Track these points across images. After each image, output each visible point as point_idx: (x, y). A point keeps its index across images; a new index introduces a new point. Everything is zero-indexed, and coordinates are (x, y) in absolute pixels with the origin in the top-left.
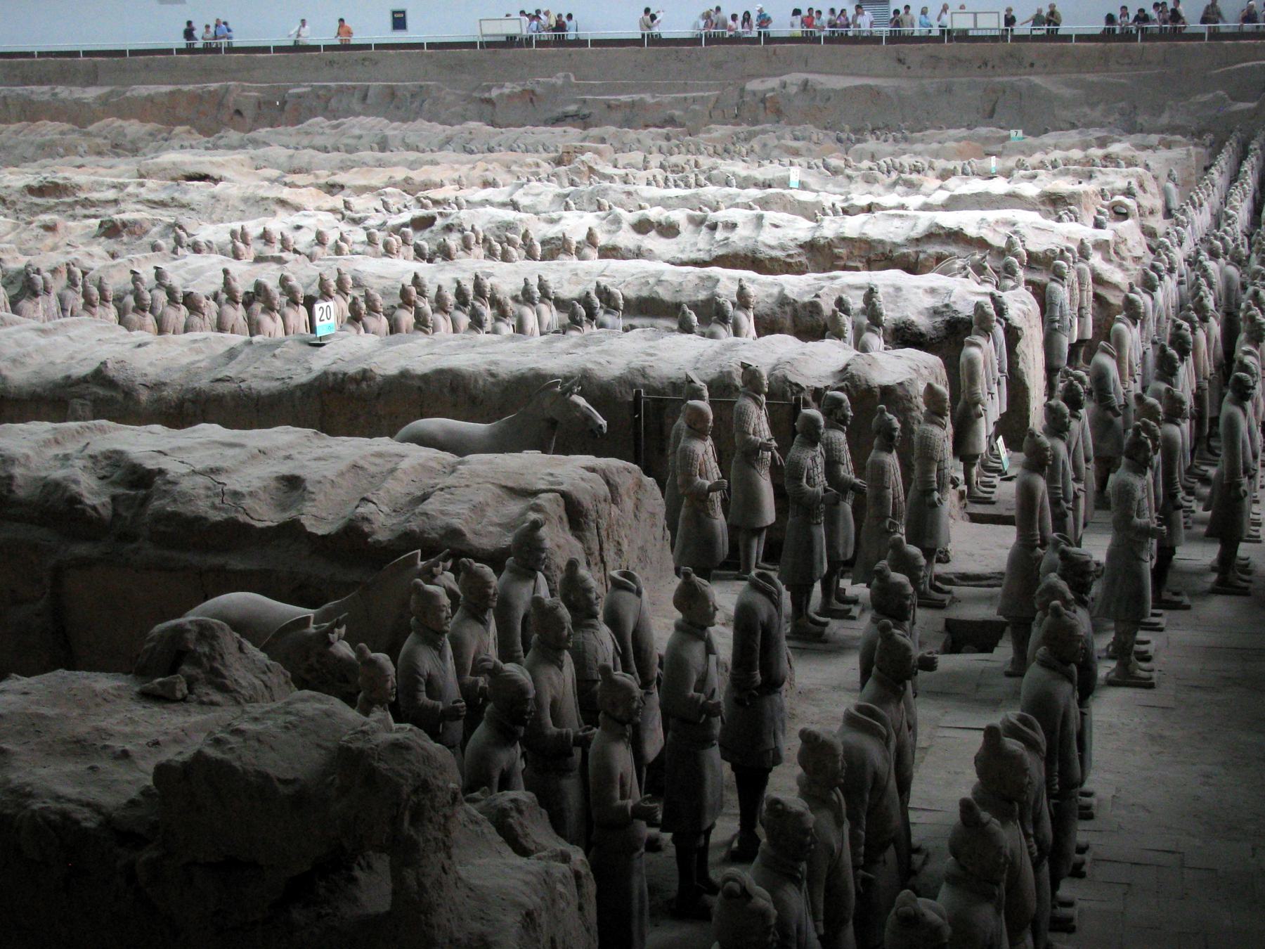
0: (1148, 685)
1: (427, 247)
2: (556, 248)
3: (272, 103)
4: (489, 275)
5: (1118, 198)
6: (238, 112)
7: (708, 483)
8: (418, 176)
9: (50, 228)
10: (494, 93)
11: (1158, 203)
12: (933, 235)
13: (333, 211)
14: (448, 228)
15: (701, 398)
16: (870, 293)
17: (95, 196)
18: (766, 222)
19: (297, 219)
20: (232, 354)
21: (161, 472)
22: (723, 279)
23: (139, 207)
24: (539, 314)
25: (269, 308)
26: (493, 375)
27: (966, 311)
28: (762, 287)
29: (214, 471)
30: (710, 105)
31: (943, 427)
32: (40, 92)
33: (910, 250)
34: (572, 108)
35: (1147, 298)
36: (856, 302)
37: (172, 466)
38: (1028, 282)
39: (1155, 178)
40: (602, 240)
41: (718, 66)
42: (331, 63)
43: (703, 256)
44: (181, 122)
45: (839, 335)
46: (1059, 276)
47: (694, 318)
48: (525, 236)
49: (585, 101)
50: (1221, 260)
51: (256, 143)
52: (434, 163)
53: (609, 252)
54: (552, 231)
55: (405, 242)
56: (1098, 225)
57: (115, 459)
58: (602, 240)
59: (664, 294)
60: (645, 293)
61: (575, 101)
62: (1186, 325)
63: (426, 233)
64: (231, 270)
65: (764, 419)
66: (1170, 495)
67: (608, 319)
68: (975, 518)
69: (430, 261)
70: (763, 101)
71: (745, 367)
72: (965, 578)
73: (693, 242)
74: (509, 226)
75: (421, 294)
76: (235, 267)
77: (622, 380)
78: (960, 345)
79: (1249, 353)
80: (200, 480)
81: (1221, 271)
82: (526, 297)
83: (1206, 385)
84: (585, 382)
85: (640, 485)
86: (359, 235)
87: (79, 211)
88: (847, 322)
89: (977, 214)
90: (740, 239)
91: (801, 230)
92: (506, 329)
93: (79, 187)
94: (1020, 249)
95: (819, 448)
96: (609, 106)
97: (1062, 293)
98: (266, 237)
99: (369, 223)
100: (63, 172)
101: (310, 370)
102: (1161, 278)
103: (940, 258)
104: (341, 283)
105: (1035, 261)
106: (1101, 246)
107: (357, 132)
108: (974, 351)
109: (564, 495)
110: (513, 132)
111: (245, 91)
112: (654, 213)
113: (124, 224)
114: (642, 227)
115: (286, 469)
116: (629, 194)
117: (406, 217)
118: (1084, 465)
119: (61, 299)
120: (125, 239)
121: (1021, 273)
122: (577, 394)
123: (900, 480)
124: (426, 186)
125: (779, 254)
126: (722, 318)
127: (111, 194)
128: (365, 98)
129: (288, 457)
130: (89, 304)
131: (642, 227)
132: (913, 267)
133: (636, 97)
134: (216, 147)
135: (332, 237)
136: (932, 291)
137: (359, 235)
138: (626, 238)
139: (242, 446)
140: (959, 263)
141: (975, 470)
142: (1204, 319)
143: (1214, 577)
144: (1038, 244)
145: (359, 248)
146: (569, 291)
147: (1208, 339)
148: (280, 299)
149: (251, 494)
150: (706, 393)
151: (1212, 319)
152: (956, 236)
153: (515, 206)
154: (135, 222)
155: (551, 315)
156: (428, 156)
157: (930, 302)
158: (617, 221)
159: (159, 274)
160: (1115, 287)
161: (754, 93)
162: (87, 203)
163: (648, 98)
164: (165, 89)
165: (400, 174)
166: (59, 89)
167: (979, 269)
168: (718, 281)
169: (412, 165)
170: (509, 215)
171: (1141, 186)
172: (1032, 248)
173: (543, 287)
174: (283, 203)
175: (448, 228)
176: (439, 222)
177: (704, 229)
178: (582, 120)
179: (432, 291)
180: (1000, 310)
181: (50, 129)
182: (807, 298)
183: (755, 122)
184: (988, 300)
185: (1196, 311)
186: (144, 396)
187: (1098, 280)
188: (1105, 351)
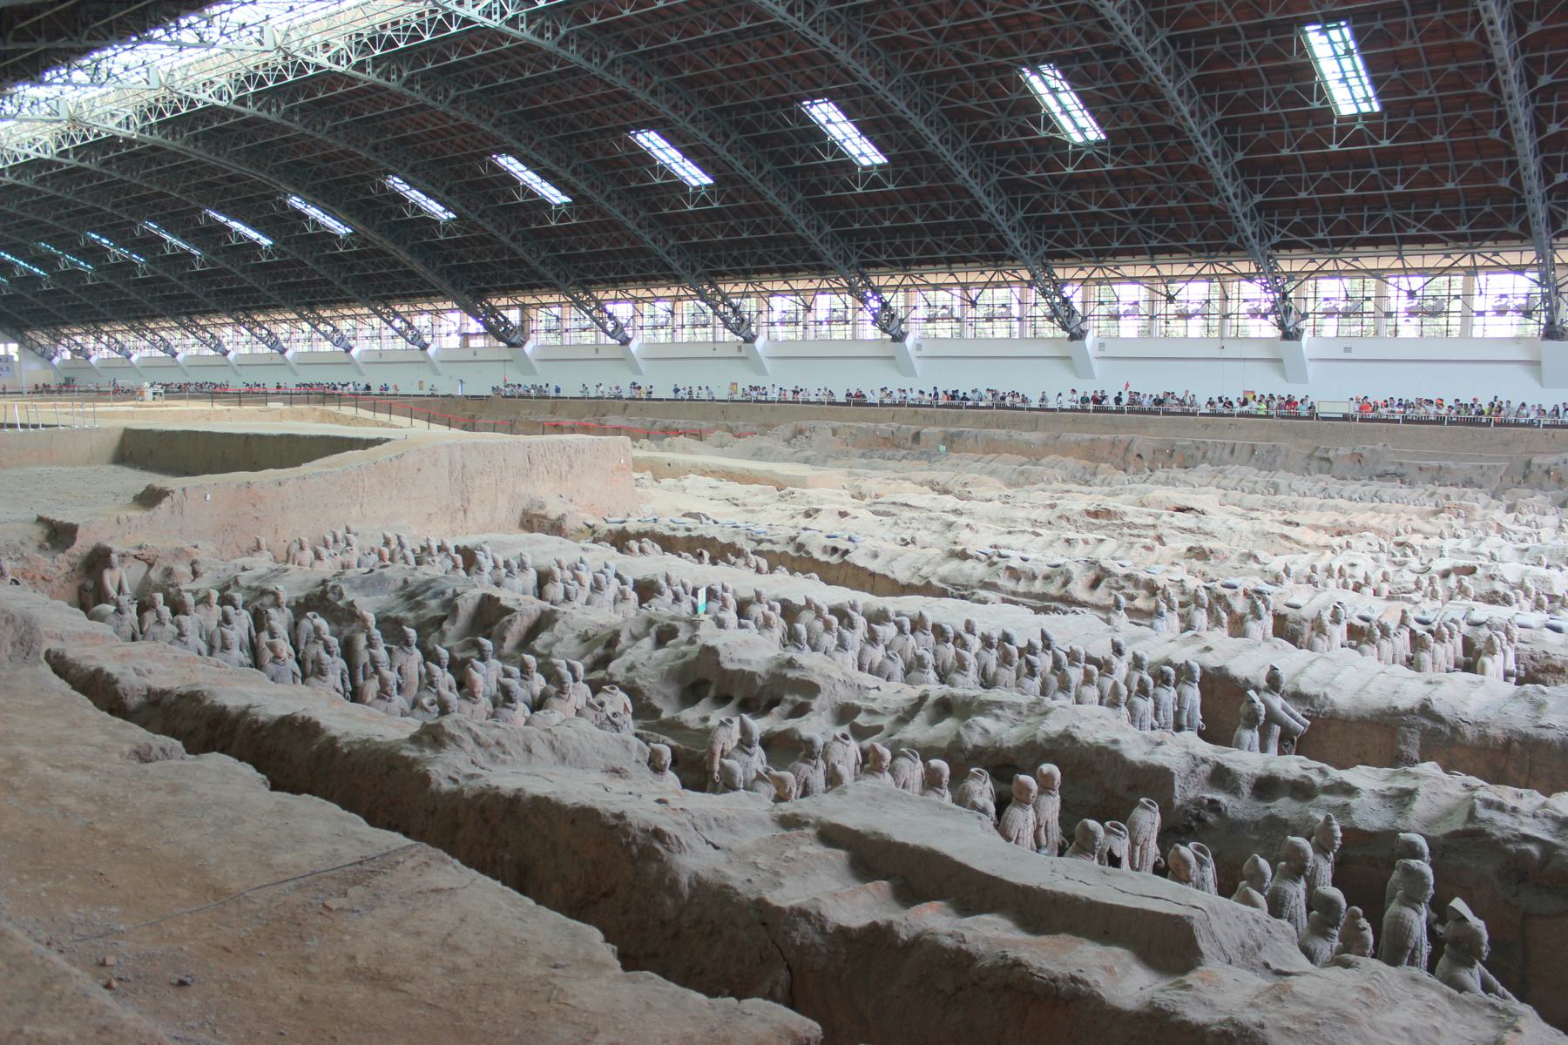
6: (1139, 456)
10: (1331, 454)
17: (1137, 521)
23: (1173, 531)
30: (1502, 473)
34: (1392, 469)
41: (1506, 444)
42: (1206, 426)
44: (1105, 460)
49: (1401, 464)
61: (1393, 463)
70: (1548, 472)
87: (1125, 530)
96: (1421, 469)
100: (1111, 504)
111: (1145, 439)
120: (1212, 562)
127: (1150, 521)
128: (1232, 452)
133: (1443, 464)
161: (1540, 466)
162: (1131, 525)
163: (1451, 464)
164: (1087, 436)
166: (1013, 433)
174: (1286, 537)
176: (1480, 571)
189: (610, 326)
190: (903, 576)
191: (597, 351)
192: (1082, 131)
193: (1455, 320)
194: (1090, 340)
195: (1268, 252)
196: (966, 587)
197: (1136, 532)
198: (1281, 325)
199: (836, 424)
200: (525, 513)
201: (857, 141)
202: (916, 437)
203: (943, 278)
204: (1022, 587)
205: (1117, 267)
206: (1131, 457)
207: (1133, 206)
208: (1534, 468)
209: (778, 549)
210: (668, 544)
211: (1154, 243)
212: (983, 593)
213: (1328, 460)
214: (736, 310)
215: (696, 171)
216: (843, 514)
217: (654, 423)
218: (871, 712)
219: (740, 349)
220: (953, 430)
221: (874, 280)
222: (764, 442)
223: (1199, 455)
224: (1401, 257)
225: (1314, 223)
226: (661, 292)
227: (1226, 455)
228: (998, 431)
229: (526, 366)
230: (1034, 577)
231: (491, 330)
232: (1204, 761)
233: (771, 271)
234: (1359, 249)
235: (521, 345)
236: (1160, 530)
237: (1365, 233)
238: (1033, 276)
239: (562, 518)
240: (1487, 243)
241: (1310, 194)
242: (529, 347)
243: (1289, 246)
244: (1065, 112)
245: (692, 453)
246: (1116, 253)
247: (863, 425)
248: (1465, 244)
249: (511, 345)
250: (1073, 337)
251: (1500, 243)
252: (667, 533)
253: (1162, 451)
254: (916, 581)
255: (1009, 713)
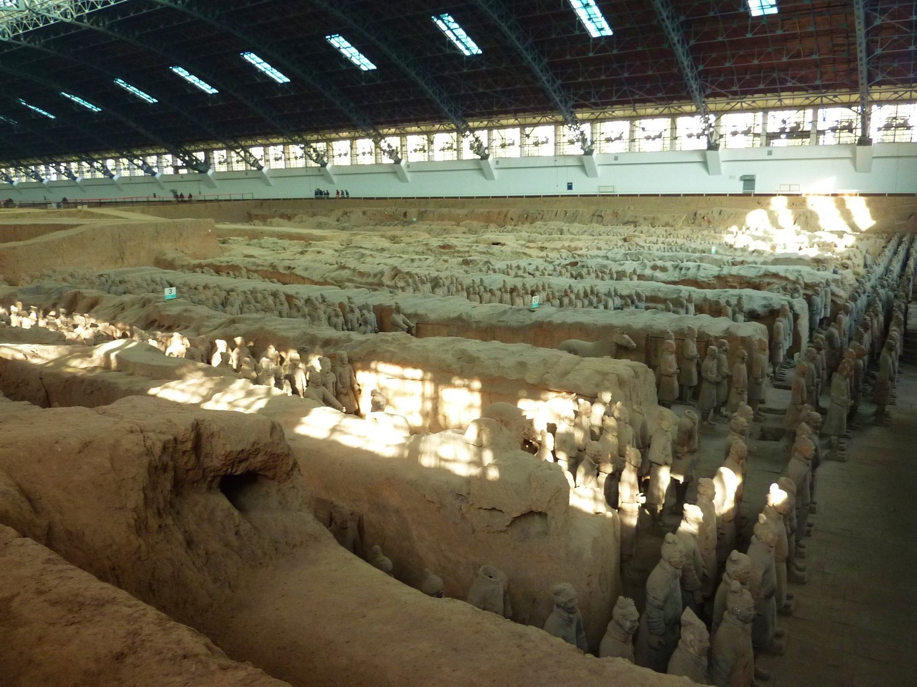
0: (842, 461)
1: (574, 273)
2: (621, 275)
3: (523, 216)
4: (596, 286)
5: (844, 261)
7: (672, 371)
8: (573, 245)
9: (446, 261)
11: (862, 263)
12: (766, 275)
13: (542, 257)
14: (583, 266)
15: (672, 339)
16: (740, 298)
17: (461, 249)
18: (701, 268)
19: (529, 260)
20: (505, 312)
21: (478, 358)
22: (683, 291)
24: (614, 301)
25: (519, 295)
26: (595, 325)
27: (777, 307)
28: (698, 293)
29: (496, 358)
31: (765, 354)
32: (445, 211)
33: (757, 280)
34: (631, 220)
35: (852, 303)
36: (734, 301)
37: (482, 356)
38: (804, 294)
39: (861, 252)
40: (638, 272)
42: (545, 202)
43: (677, 280)
45: (727, 315)
46: (817, 294)
47: (671, 306)
48: (610, 270)
50: (886, 289)
51: (518, 231)
52: (579, 240)
53: (641, 277)
54: (620, 269)
55: (567, 271)
56: (835, 272)
57: (463, 352)
58: (638, 272)
59: (660, 295)
60: (653, 294)
62: (868, 318)
63: (575, 268)
64: (507, 281)
65: (695, 346)
66: (857, 386)
67: (639, 304)
68: (776, 387)
69: (576, 279)
71: (689, 328)
72: (770, 411)
73: (674, 275)
74: (605, 266)
75: (572, 292)
76: (507, 278)
77: (642, 329)
78: (774, 321)
79: (895, 330)
80: (491, 361)
81: (886, 293)
82: (608, 295)
83: (876, 341)
84: (627, 329)
85: (647, 372)
86: (551, 267)
88: (730, 310)
89: (785, 267)
90: (691, 274)
91: (714, 270)
92: (601, 307)
93: (456, 246)
94: (802, 282)
95: (715, 360)
96: (645, 219)
97: (818, 300)
98: (518, 267)
99: (555, 263)
100: (452, 241)
101: (531, 320)
102: (859, 296)
103: (769, 284)
104: (543, 286)
105: (807, 286)
106: (836, 281)
107: (553, 227)
108: (780, 323)
109: (618, 375)
110: (609, 228)
111: (513, 212)
112: (659, 263)
113: (471, 261)
114: (654, 268)
115: (521, 359)
116: (650, 254)
117: (568, 262)
118: (821, 371)
119: (448, 288)
121: (802, 291)
122: (627, 334)
123: (746, 375)
124: (576, 249)
125: (704, 279)
126: (682, 306)
127: (467, 249)
129: (522, 355)
130: (457, 291)
131: (654, 268)
132: (757, 287)
134: (503, 232)
135: (541, 268)
136: (765, 298)
137: (551, 267)
138: (648, 272)
139: (507, 350)
140: (776, 286)
141: (777, 368)
142: (877, 315)
143: (873, 419)
144: (808, 280)
145: (551, 273)
146: (625, 292)
147: (878, 322)
148: (522, 292)
149: (509, 368)
150: (674, 337)
151: (880, 315)
152: (775, 275)
153: (607, 258)
154: (474, 260)
155: (618, 301)
156: (577, 237)
157: (764, 302)
158: (645, 266)
159: (481, 280)
160: (840, 297)
162: (459, 252)
165: (566, 244)
167: (785, 289)
168: (681, 291)
169: (571, 240)
170: (606, 262)
171: (855, 255)
172: (806, 281)
173: (615, 291)
174: (525, 254)
175: (583, 266)
176: (580, 264)
177: (677, 269)
178: (635, 224)
179: (576, 291)
180: (791, 308)
181: (448, 224)
182: (715, 299)
183: (700, 225)
184: (786, 303)
185: (873, 311)
186: (474, 326)
187: (833, 294)
188: (834, 327)
189: (252, 160)
190: (316, 278)
191: (247, 174)
192: (467, 48)
193: (668, 142)
194: (490, 159)
195: (571, 110)
196: (341, 282)
197: (460, 255)
198: (582, 148)
199: (365, 209)
200: (156, 258)
201: (358, 57)
202: (405, 214)
203: (414, 129)
204: (364, 280)
205: (499, 121)
206: (508, 220)
207: (499, 89)
208: (698, 215)
209: (264, 269)
210: (218, 270)
211: (514, 107)
212: (347, 284)
213: (601, 216)
214: (315, 150)
215: (280, 74)
216: (319, 252)
217: (276, 212)
218: (208, 327)
219: (319, 171)
220: (423, 210)
221: (381, 131)
222: (323, 219)
223: (540, 217)
224: (635, 110)
225: (590, 93)
226: (275, 141)
227: (553, 217)
228: (445, 209)
229: (209, 183)
230: (370, 275)
231: (188, 165)
232: (308, 334)
233: (329, 128)
234: (614, 106)
235: (206, 172)
236: (470, 254)
237: (614, 99)
238: (457, 127)
239: (173, 260)
240: (675, 102)
241: (585, 78)
242: (210, 172)
243: (582, 106)
244: (458, 39)
245: (281, 226)
246: (497, 113)
247: (379, 209)
248: (664, 102)
249: (200, 172)
250: (482, 158)
251: (682, 101)
252: (218, 264)
253: (523, 216)
254: (321, 280)
255: (250, 322)
